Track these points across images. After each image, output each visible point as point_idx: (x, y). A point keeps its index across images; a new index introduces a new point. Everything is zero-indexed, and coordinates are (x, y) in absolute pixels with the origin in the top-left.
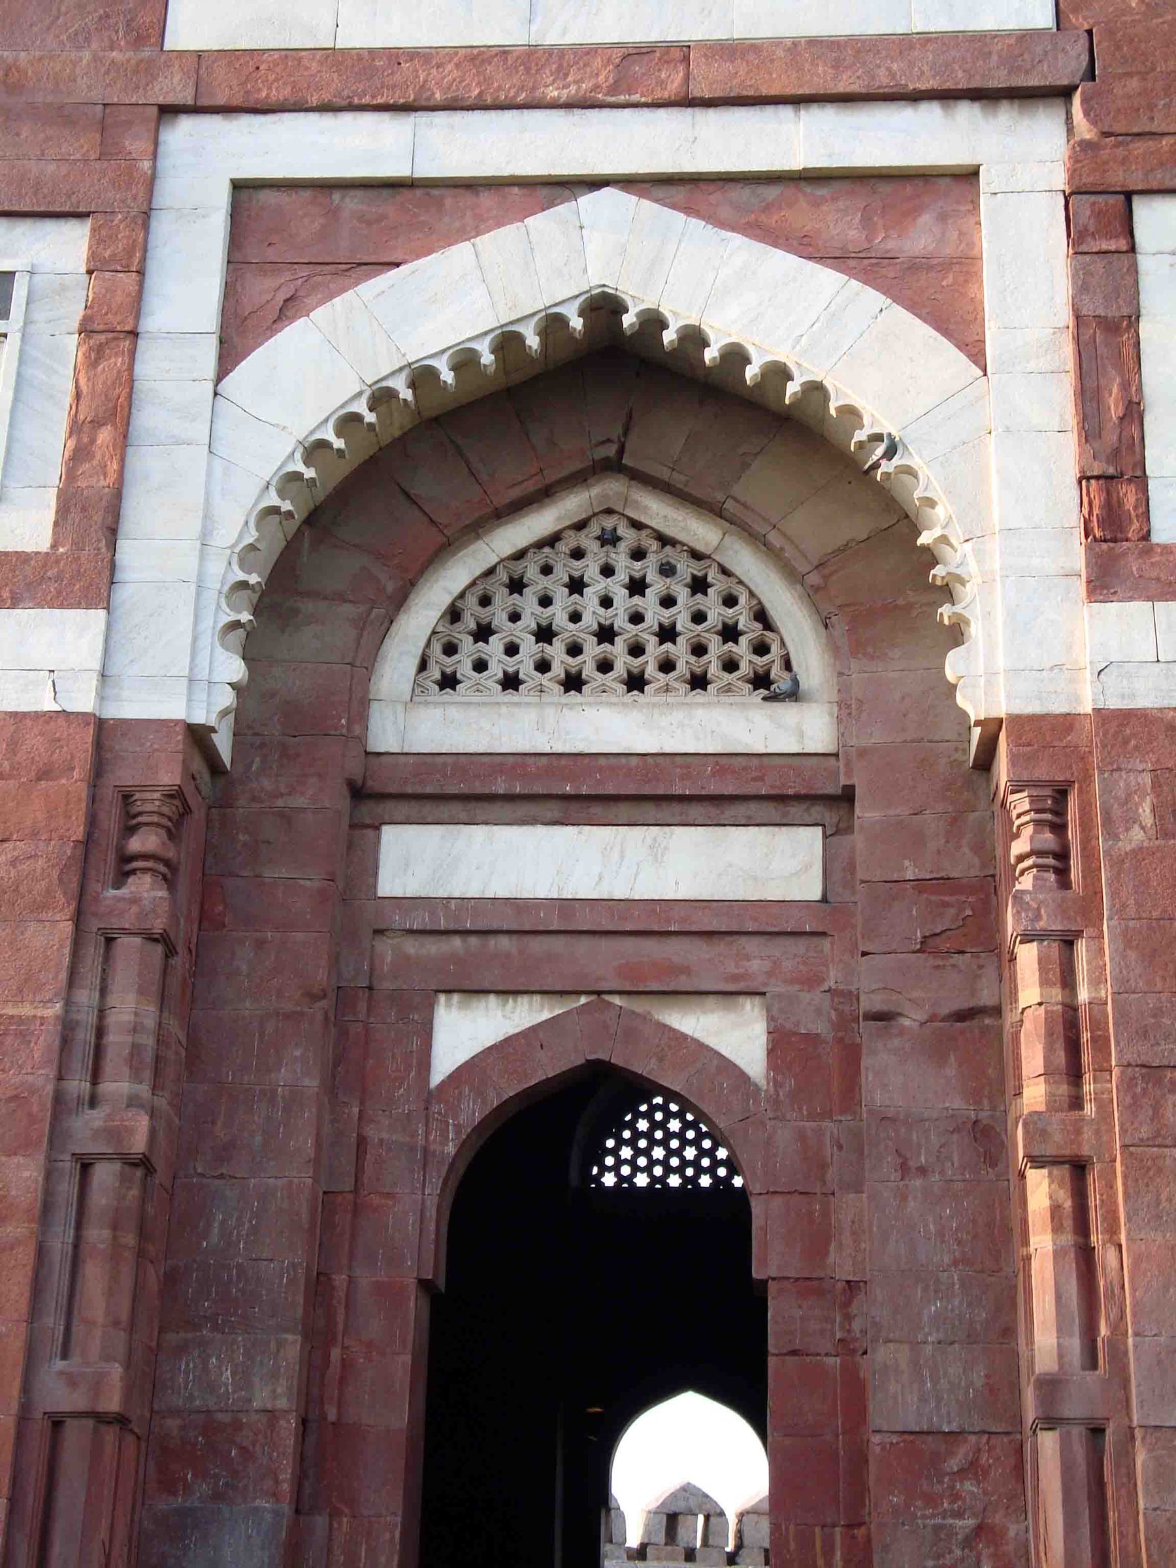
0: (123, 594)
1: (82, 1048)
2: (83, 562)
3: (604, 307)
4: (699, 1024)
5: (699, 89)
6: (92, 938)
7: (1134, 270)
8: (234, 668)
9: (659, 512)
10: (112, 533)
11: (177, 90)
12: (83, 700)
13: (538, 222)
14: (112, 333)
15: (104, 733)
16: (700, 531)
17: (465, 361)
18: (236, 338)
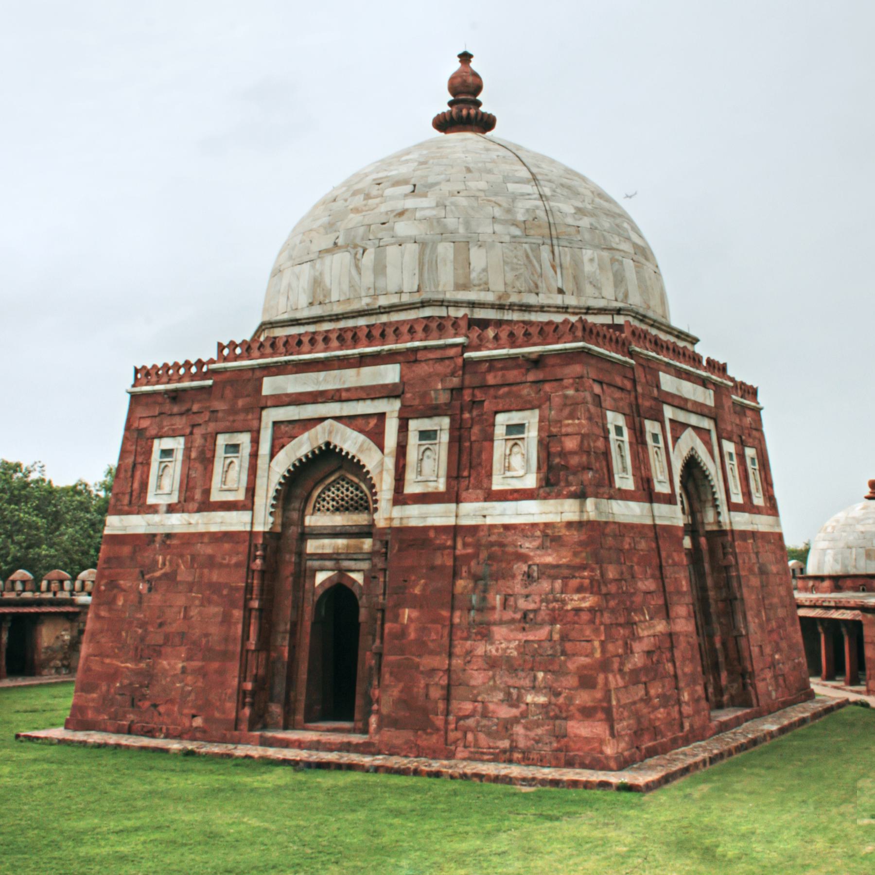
0: (256, 507)
1: (249, 589)
2: (248, 504)
3: (328, 444)
4: (353, 575)
5: (343, 398)
6: (250, 571)
7: (407, 435)
8: (271, 519)
9: (351, 477)
10: (253, 496)
11: (263, 403)
12: (248, 529)
13: (319, 427)
14: (254, 455)
15: (251, 533)
16: (356, 480)
17: (306, 456)
18: (272, 455)
